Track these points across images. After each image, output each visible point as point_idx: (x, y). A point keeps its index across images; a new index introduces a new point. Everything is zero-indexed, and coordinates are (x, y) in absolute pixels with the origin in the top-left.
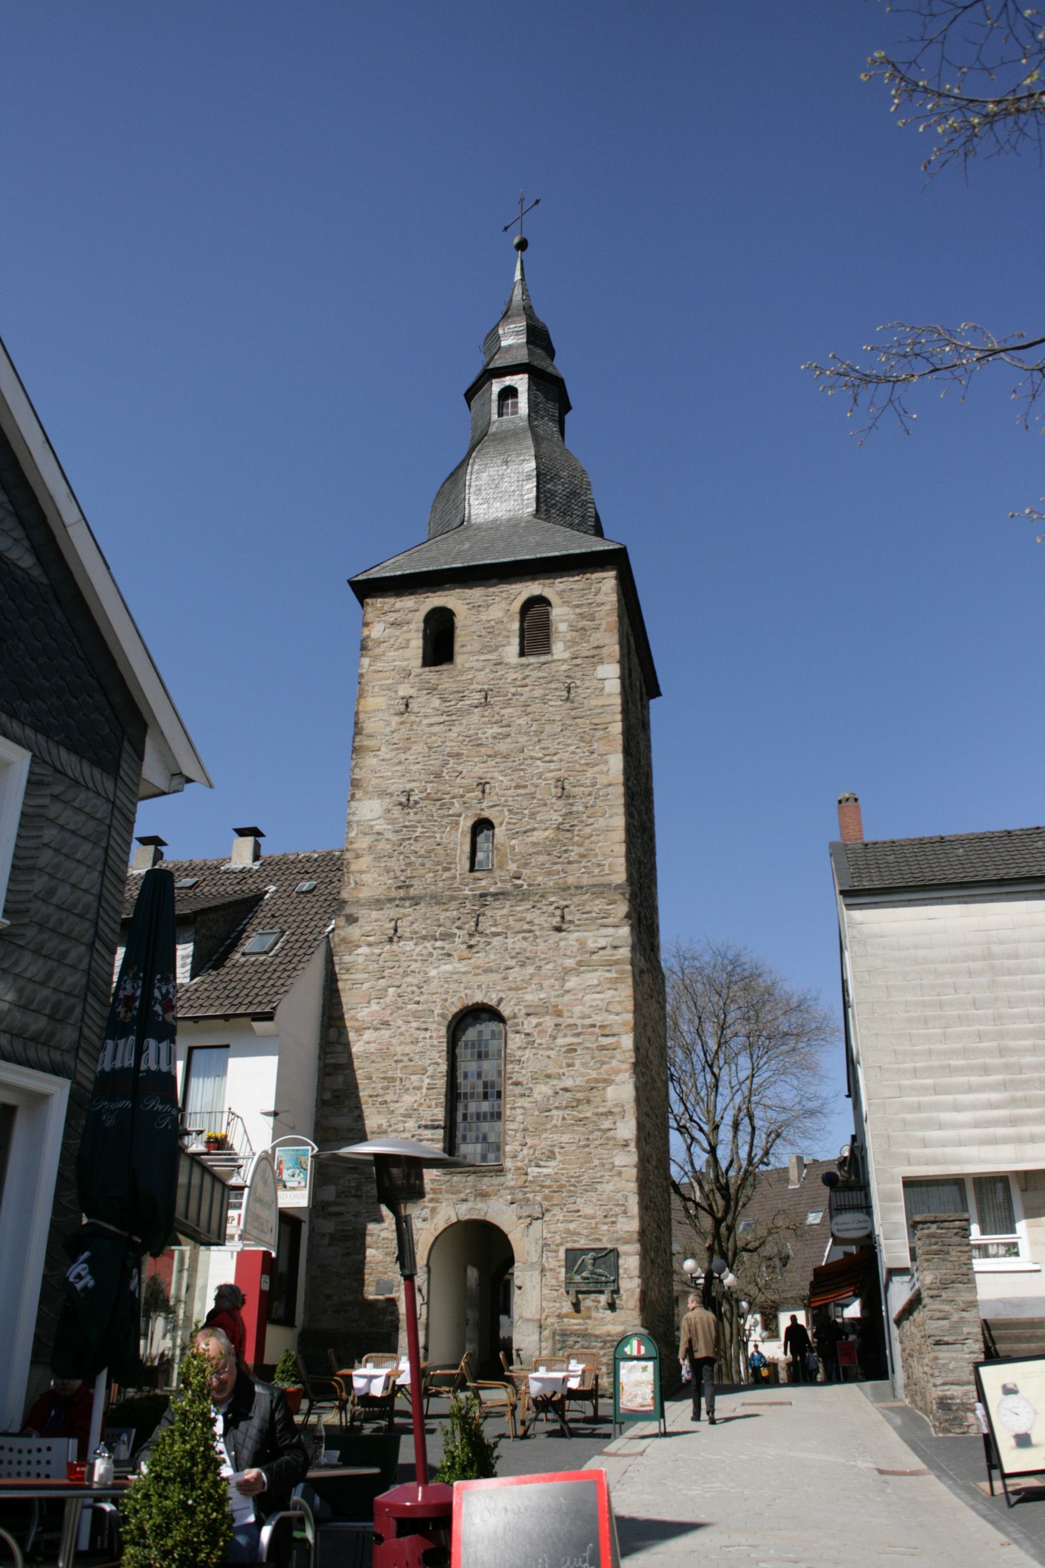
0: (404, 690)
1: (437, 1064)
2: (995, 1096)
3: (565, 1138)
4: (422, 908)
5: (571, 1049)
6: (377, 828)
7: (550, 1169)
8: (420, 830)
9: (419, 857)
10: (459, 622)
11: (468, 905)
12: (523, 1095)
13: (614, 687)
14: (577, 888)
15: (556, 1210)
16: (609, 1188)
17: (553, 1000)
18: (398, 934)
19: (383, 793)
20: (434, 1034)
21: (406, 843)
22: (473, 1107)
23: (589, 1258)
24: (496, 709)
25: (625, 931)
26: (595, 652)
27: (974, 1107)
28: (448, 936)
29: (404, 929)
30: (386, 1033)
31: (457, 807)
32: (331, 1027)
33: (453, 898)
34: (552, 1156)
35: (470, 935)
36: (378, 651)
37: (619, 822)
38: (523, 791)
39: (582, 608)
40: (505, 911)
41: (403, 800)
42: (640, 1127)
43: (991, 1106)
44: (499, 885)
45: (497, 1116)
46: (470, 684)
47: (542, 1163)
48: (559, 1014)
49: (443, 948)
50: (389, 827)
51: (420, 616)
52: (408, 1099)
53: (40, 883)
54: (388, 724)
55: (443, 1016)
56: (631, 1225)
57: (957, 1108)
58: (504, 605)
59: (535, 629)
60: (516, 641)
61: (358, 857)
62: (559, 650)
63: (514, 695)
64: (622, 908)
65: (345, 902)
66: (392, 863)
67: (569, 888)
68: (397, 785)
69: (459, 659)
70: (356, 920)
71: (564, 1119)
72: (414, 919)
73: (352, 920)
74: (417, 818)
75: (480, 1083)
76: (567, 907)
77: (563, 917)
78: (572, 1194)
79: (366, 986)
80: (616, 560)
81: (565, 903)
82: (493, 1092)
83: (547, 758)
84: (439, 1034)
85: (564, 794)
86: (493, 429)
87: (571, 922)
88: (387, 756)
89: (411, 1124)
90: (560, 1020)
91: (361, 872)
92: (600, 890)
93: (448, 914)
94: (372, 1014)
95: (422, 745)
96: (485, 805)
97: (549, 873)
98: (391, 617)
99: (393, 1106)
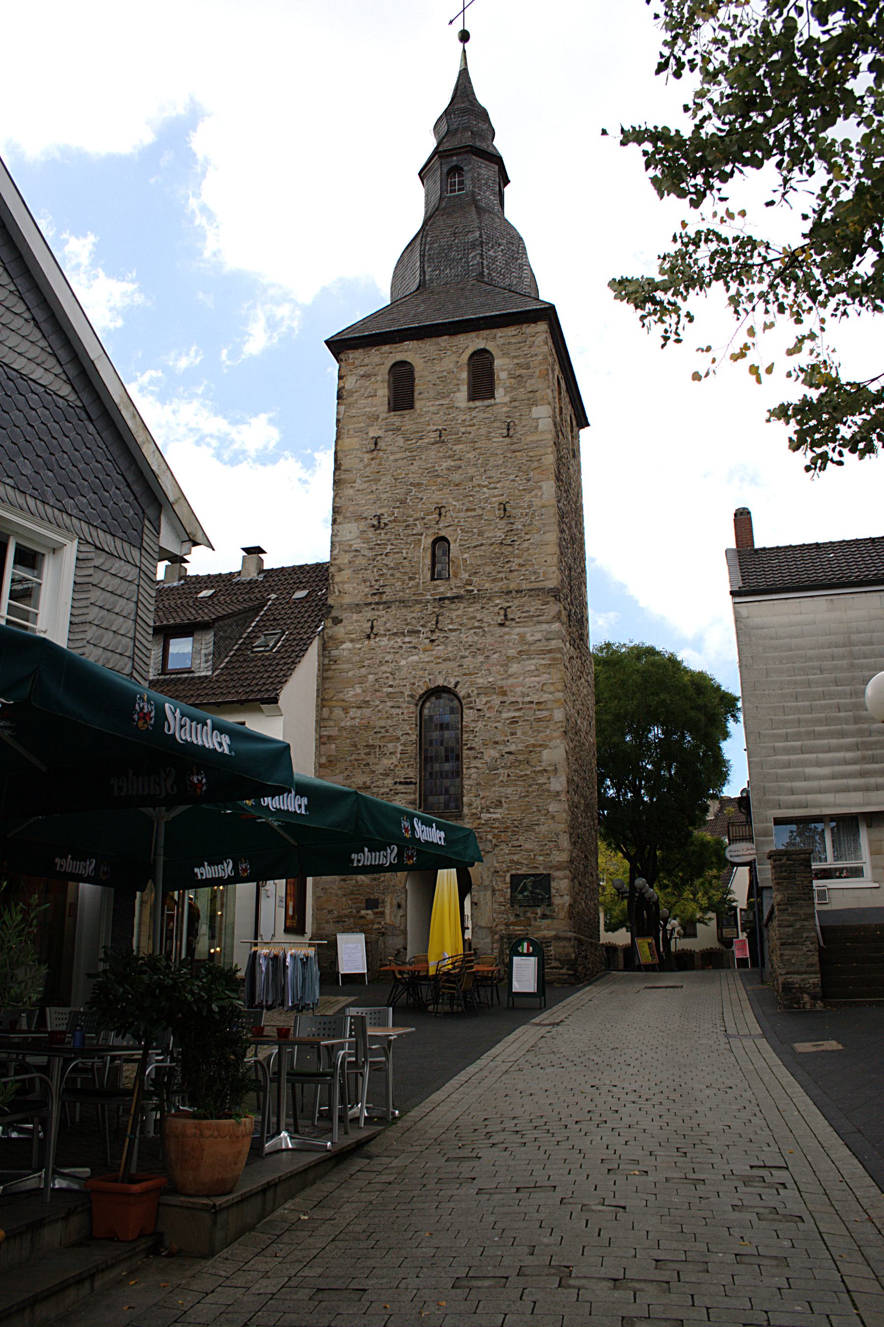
1: (408, 734)
2: (849, 755)
3: (509, 790)
4: (393, 610)
5: (514, 721)
6: (355, 547)
8: (389, 547)
9: (390, 569)
11: (430, 607)
12: (476, 758)
14: (517, 592)
15: (503, 846)
16: (544, 828)
17: (500, 683)
18: (375, 631)
19: (360, 518)
20: (405, 711)
21: (379, 558)
22: (437, 767)
23: (529, 882)
24: (450, 446)
26: (531, 395)
27: (832, 763)
28: (414, 632)
29: (380, 628)
30: (367, 712)
32: (324, 706)
33: (418, 602)
34: (499, 804)
35: (432, 631)
36: (351, 400)
38: (473, 514)
40: (459, 612)
41: (376, 523)
42: (570, 781)
43: (846, 762)
44: (454, 591)
45: (458, 773)
46: (429, 425)
47: (491, 810)
48: (504, 693)
49: (410, 642)
50: (365, 545)
52: (386, 762)
53: (91, 632)
54: (362, 461)
55: (412, 696)
57: (819, 764)
58: (454, 358)
59: (482, 378)
60: (464, 388)
61: (340, 570)
62: (499, 393)
63: (463, 433)
65: (331, 607)
66: (368, 574)
67: (511, 592)
68: (370, 511)
69: (418, 404)
70: (341, 621)
71: (509, 776)
72: (387, 619)
73: (337, 621)
74: (387, 537)
75: (442, 749)
76: (509, 607)
77: (505, 615)
78: (514, 833)
79: (350, 674)
81: (508, 605)
82: (454, 755)
83: (492, 486)
84: (409, 710)
87: (512, 619)
88: (361, 487)
89: (389, 781)
90: (505, 699)
91: (343, 583)
93: (414, 615)
94: (355, 695)
95: (389, 477)
96: (441, 525)
97: (494, 580)
99: (373, 768)
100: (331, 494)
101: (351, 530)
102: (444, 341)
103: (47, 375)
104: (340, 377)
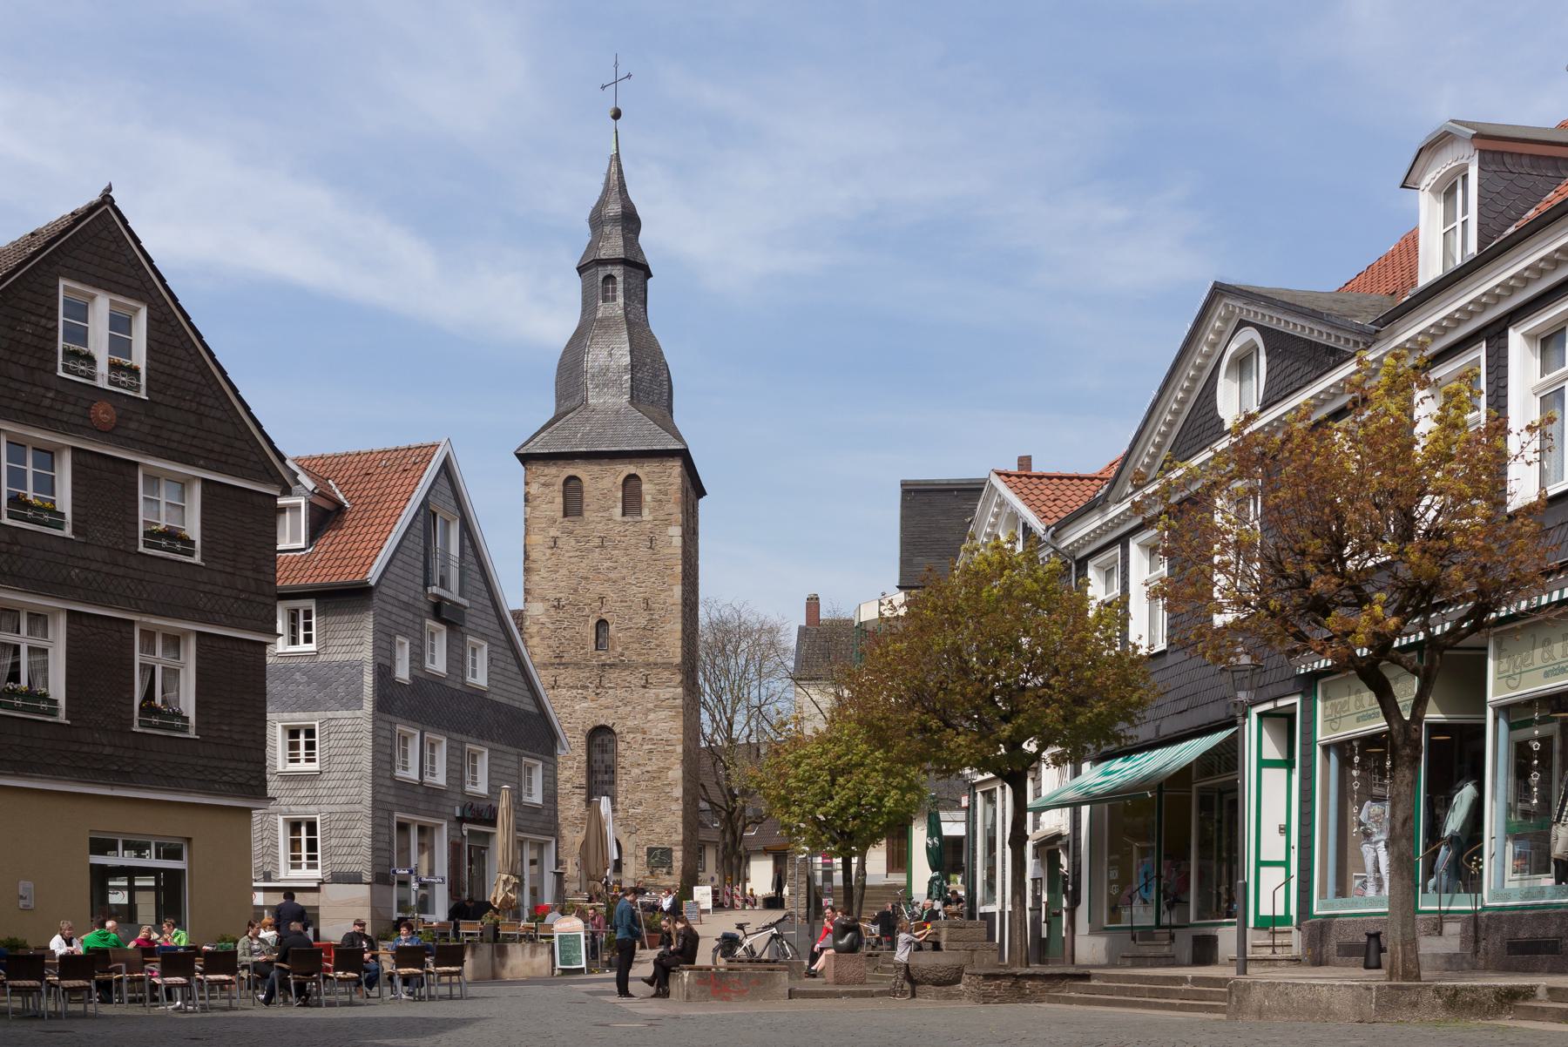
0: (553, 532)
4: (570, 670)
19: (544, 599)
22: (600, 777)
25: (680, 690)
28: (585, 687)
29: (561, 682)
37: (679, 627)
39: (659, 482)
42: (685, 790)
45: (613, 782)
51: (561, 481)
56: (678, 837)
59: (631, 493)
60: (620, 505)
62: (646, 512)
64: (679, 678)
66: (551, 642)
68: (552, 595)
69: (586, 514)
72: (566, 676)
80: (684, 456)
82: (611, 770)
85: (648, 608)
86: (599, 315)
92: (667, 666)
98: (542, 480)
100: (522, 579)
103: (532, 708)
104: (526, 484)
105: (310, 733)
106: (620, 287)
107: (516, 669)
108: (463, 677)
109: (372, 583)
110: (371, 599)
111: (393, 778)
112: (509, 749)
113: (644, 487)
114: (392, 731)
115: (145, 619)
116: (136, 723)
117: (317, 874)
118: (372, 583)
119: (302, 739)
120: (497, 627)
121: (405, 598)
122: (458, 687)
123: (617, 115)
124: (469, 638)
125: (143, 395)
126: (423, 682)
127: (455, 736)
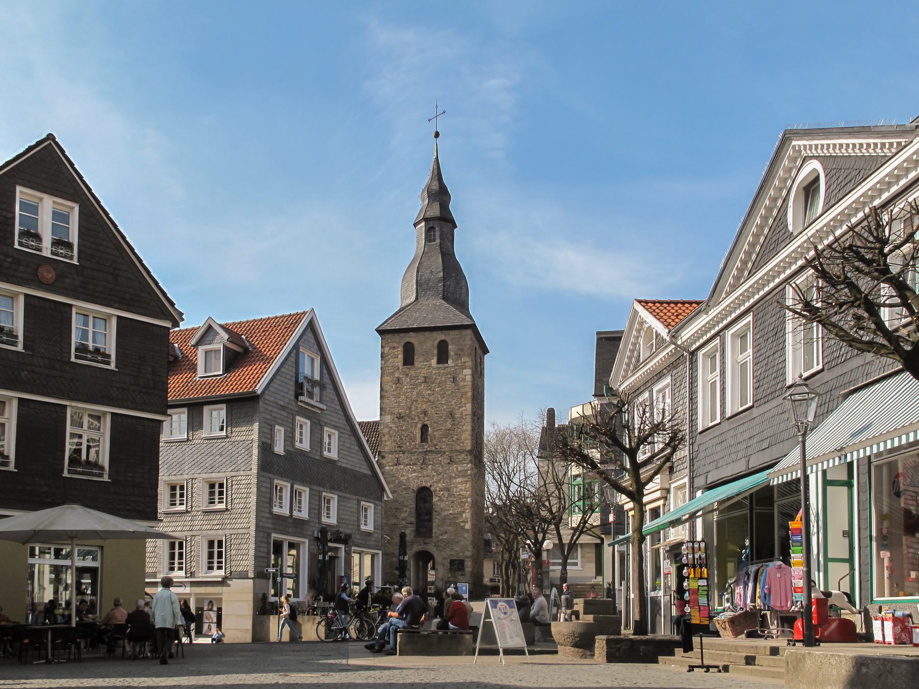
7: (445, 537)
10: (416, 347)
13: (469, 378)
19: (391, 414)
22: (422, 517)
31: (416, 420)
34: (446, 533)
37: (469, 428)
45: (430, 520)
52: (403, 515)
62: (450, 361)
64: (469, 458)
68: (396, 411)
69: (416, 364)
80: (473, 327)
84: (413, 496)
89: (404, 522)
92: (461, 452)
98: (391, 345)
101: (388, 418)
102: (427, 334)
103: (368, 472)
104: (382, 347)
105: (221, 486)
106: (438, 233)
107: (357, 448)
108: (321, 452)
109: (259, 392)
110: (258, 403)
111: (271, 512)
112: (352, 496)
113: (450, 347)
114: (271, 484)
115: (74, 404)
116: (66, 471)
117: (222, 573)
118: (259, 392)
119: (217, 490)
120: (345, 423)
121: (281, 403)
122: (318, 458)
123: (437, 135)
124: (326, 428)
125: (75, 262)
126: (293, 454)
127: (315, 487)
